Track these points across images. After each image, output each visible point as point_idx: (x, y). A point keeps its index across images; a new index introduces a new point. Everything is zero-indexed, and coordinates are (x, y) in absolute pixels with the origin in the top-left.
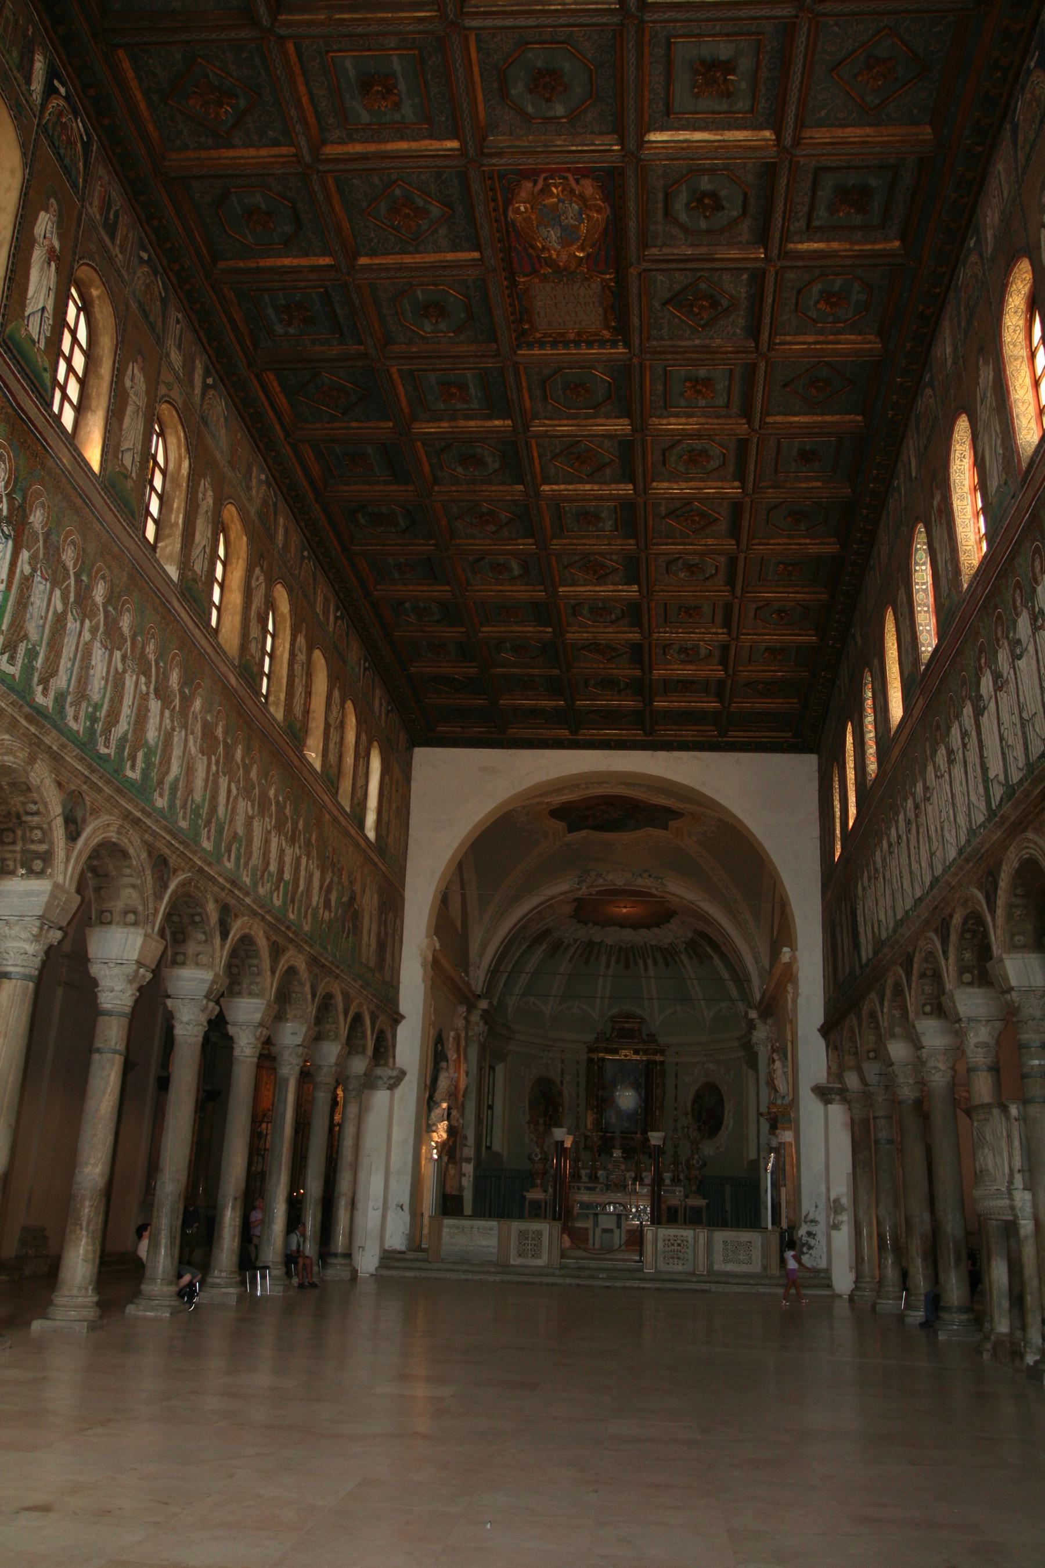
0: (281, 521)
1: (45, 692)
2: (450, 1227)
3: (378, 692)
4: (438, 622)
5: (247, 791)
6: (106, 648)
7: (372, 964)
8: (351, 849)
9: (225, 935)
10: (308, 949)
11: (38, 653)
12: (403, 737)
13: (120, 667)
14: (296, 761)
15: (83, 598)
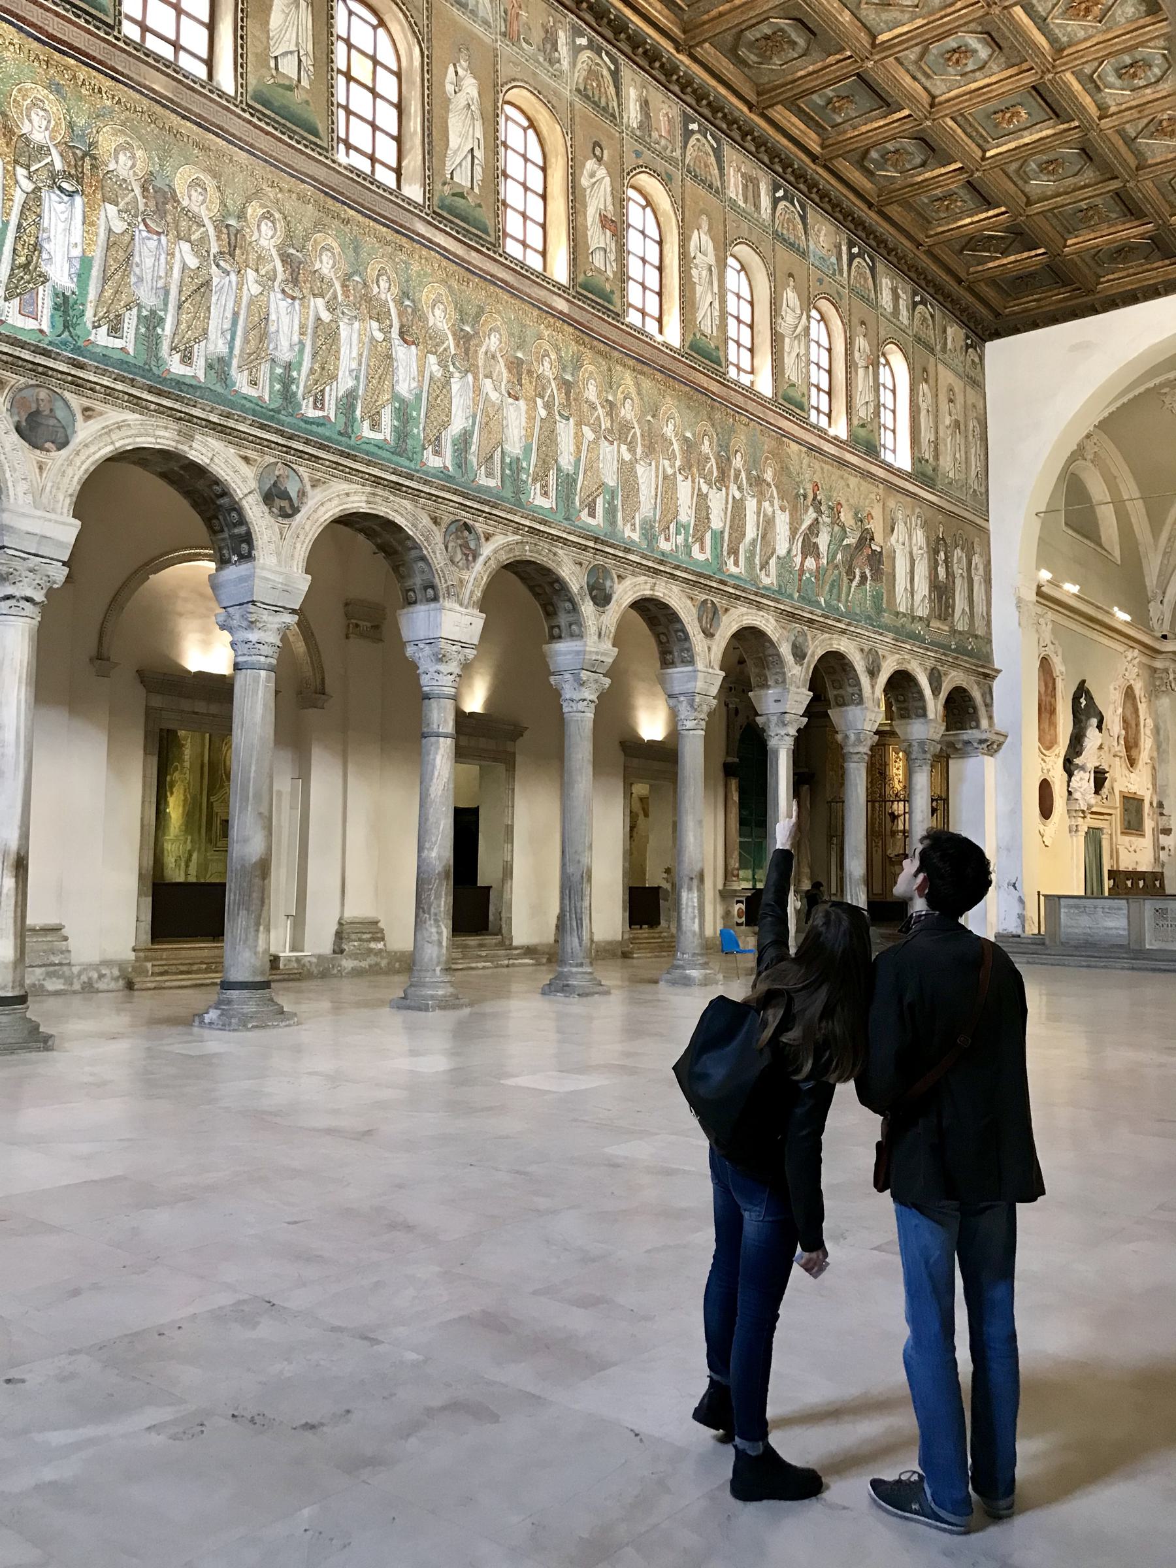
0: (632, 94)
1: (187, 358)
2: (1070, 907)
3: (886, 283)
4: (923, 165)
5: (621, 433)
6: (293, 298)
7: (922, 611)
8: (854, 481)
9: (602, 598)
10: (772, 604)
11: (162, 320)
12: (955, 334)
13: (326, 316)
14: (714, 387)
15: (234, 245)
